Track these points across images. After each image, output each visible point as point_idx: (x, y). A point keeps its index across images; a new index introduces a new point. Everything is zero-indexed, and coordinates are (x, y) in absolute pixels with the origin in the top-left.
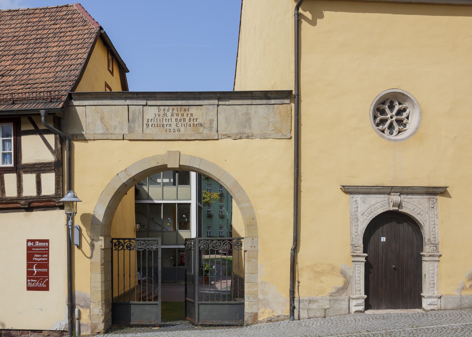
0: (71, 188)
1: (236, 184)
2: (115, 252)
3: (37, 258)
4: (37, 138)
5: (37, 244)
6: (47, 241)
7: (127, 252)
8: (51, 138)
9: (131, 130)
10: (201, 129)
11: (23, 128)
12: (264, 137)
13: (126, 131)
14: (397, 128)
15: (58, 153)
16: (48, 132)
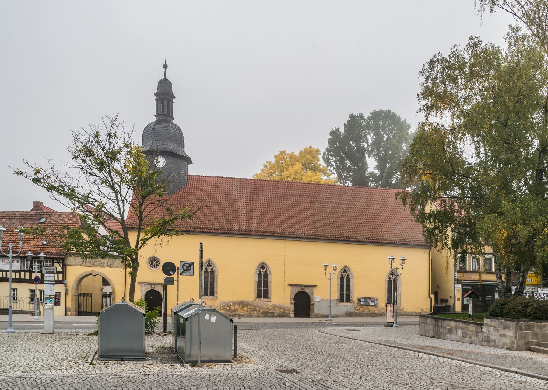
0: (66, 279)
1: (110, 280)
2: (80, 297)
3: (57, 297)
4: (58, 264)
5: (57, 293)
6: (60, 293)
7: (89, 297)
8: (61, 265)
9: (82, 264)
10: (101, 264)
11: (54, 261)
12: (117, 267)
13: (81, 264)
14: (153, 266)
15: (63, 269)
16: (61, 263)
